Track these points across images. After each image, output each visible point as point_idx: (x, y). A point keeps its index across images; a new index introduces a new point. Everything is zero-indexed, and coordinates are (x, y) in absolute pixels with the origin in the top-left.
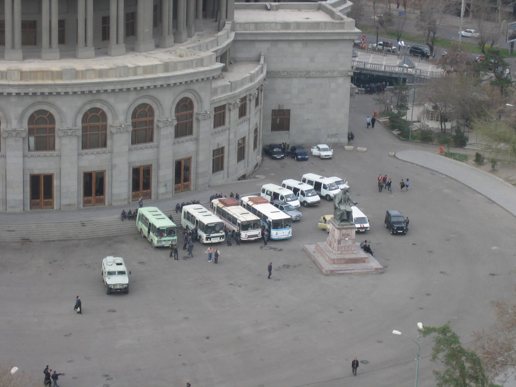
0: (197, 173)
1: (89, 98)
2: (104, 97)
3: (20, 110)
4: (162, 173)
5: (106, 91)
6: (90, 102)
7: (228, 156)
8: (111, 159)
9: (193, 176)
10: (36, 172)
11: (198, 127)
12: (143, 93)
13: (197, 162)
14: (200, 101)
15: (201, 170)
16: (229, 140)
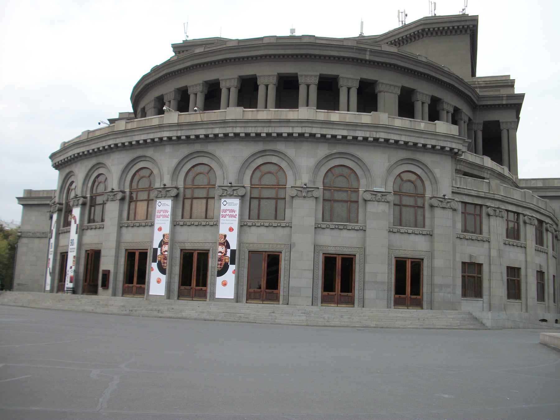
0: (432, 285)
1: (260, 147)
2: (280, 146)
3: (175, 162)
4: (369, 268)
5: (279, 135)
6: (262, 153)
7: (490, 280)
8: (290, 236)
9: (425, 288)
10: (188, 246)
11: (432, 218)
12: (340, 149)
13: (432, 268)
14: (435, 181)
15: (438, 280)
16: (490, 256)
